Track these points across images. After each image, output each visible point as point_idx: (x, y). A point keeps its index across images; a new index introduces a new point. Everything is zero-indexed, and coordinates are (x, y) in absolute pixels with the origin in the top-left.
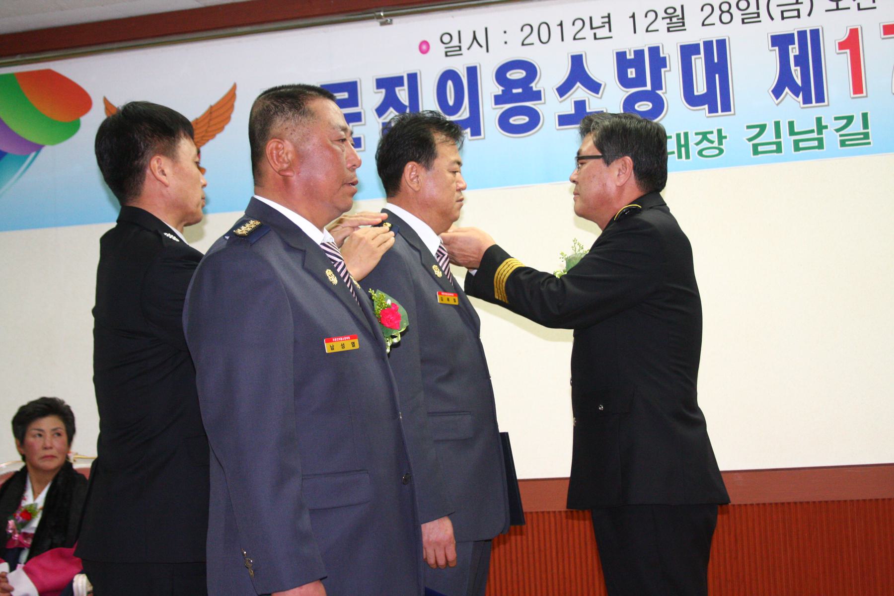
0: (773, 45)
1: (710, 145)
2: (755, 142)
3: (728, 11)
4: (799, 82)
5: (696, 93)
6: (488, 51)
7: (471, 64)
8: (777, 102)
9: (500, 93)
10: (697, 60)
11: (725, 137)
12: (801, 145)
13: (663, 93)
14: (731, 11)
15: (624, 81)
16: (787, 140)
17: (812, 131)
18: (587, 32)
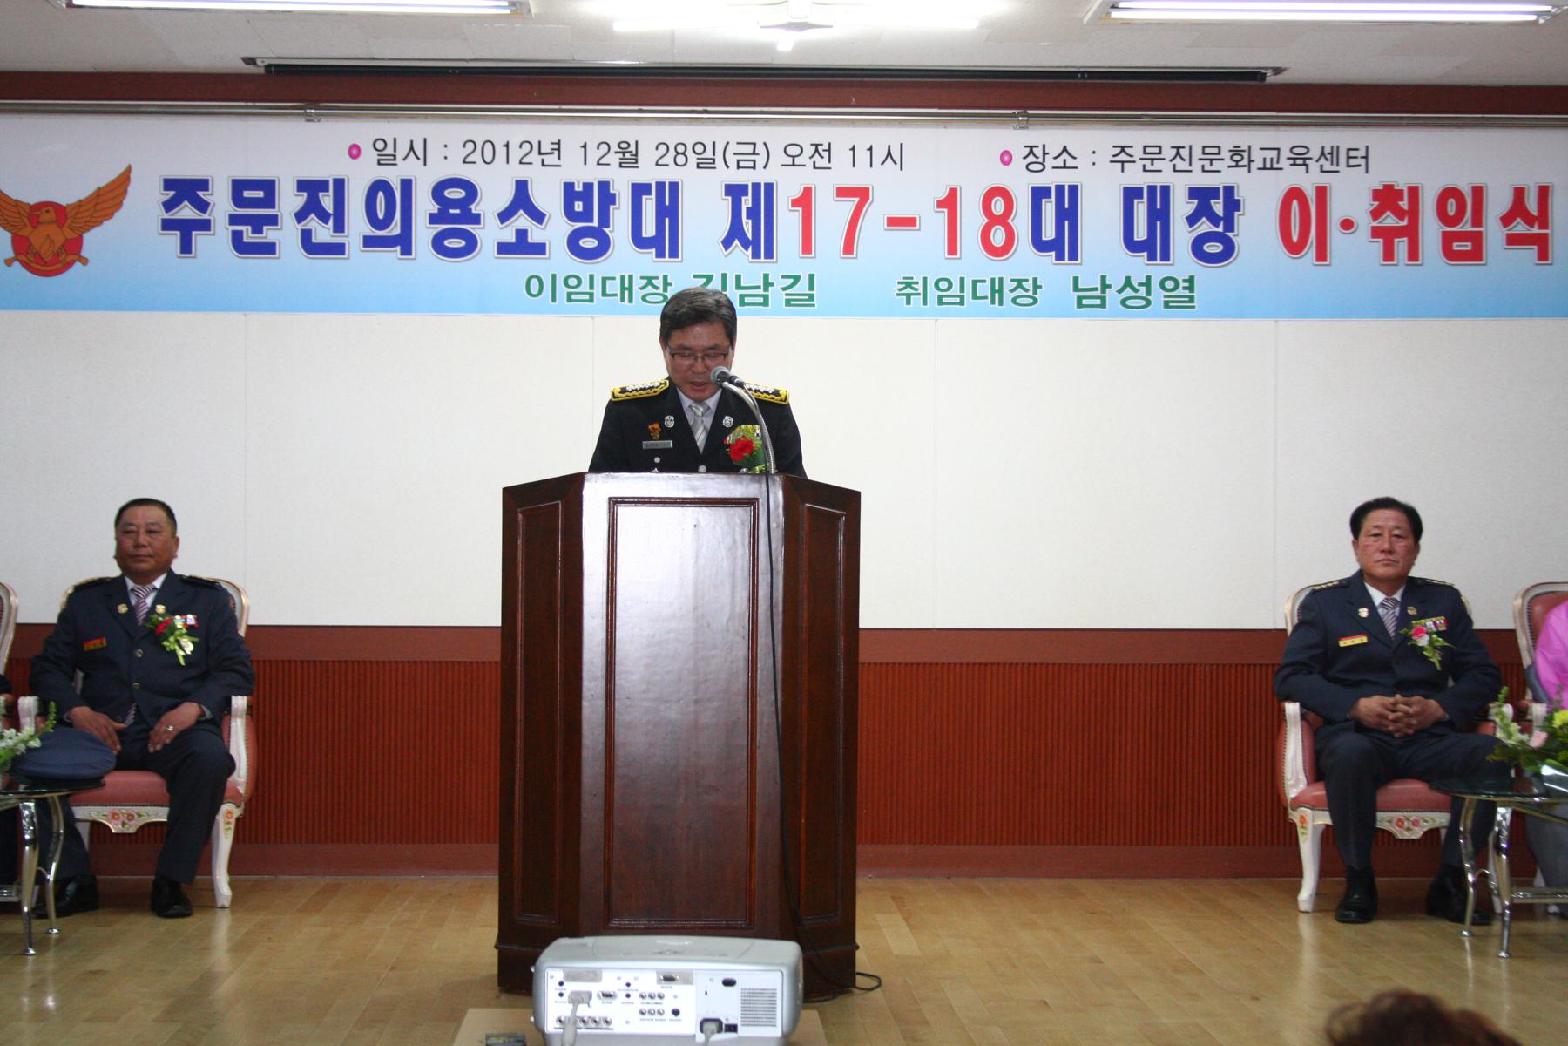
0: (726, 195)
1: (655, 291)
3: (683, 154)
4: (749, 235)
5: (644, 235)
6: (425, 164)
8: (726, 253)
9: (436, 211)
11: (671, 284)
12: (747, 300)
13: (611, 232)
14: (686, 153)
15: (571, 214)
17: (759, 287)
18: (535, 157)
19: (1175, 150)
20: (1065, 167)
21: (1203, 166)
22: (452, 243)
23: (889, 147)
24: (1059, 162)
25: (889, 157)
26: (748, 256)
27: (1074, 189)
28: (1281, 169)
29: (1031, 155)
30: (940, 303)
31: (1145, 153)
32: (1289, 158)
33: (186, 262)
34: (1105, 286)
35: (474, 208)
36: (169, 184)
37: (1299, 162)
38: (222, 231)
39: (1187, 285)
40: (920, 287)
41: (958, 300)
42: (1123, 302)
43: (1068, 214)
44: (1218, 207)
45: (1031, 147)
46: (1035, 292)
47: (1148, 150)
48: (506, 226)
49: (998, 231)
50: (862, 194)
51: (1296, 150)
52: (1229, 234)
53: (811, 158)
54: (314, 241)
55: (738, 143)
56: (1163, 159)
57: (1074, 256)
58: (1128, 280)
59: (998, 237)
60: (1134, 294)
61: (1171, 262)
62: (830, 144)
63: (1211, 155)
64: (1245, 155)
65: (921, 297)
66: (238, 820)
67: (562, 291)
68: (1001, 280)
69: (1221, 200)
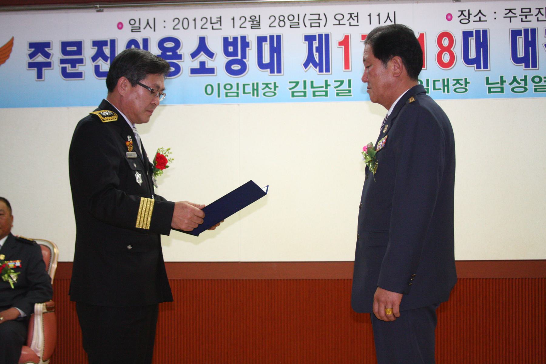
0: (305, 40)
1: (269, 90)
2: (293, 90)
3: (283, 21)
4: (317, 61)
5: (264, 62)
6: (154, 31)
7: (145, 37)
8: (306, 70)
9: (160, 54)
12: (317, 94)
14: (285, 21)
15: (227, 53)
16: (309, 91)
17: (323, 87)
18: (208, 25)
19: (538, 10)
20: (480, 21)
23: (388, 13)
24: (477, 18)
25: (388, 19)
26: (317, 71)
27: (485, 32)
29: (462, 15)
31: (522, 12)
33: (40, 83)
34: (502, 81)
35: (179, 52)
36: (31, 45)
38: (57, 67)
42: (513, 90)
45: (462, 11)
46: (466, 86)
47: (524, 11)
48: (195, 60)
49: (446, 55)
53: (348, 20)
54: (101, 70)
55: (311, 14)
56: (532, 15)
57: (486, 66)
58: (515, 79)
59: (446, 58)
62: (358, 13)
67: (223, 91)
68: (448, 80)
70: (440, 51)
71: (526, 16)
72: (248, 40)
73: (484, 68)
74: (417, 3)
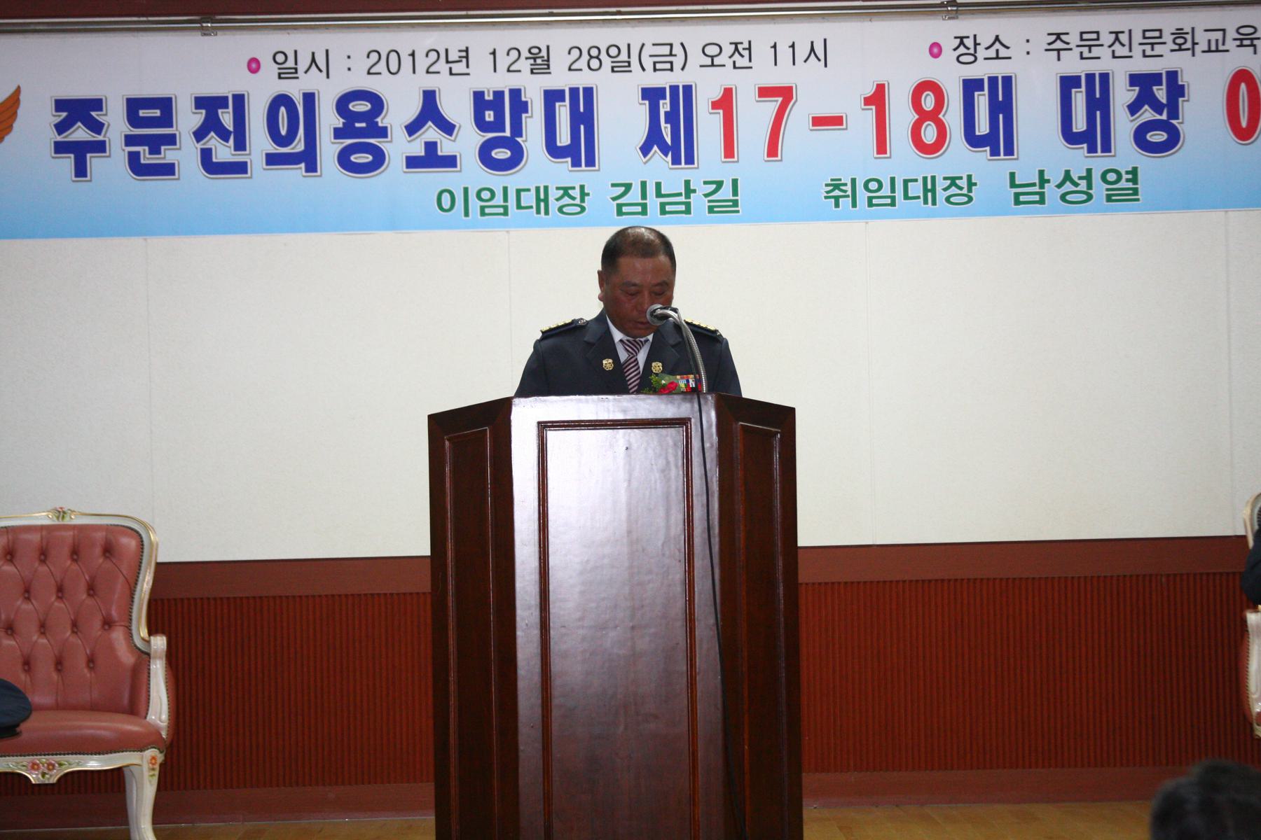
0: (643, 99)
1: (572, 202)
2: (620, 201)
3: (597, 57)
4: (669, 140)
5: (559, 144)
6: (328, 77)
7: (309, 89)
8: (644, 160)
9: (341, 126)
10: (562, 108)
11: (588, 194)
13: (523, 141)
14: (600, 57)
15: (481, 124)
17: (680, 195)
18: (442, 66)
19: (1114, 35)
20: (997, 58)
21: (1144, 51)
22: (358, 158)
23: (812, 43)
24: (992, 53)
25: (812, 54)
26: (668, 162)
27: (1008, 80)
28: (1227, 51)
29: (962, 47)
30: (870, 204)
31: (1082, 40)
32: (1235, 39)
33: (82, 186)
34: (1043, 181)
36: (60, 105)
37: (1247, 42)
38: (118, 152)
39: (1130, 176)
40: (849, 188)
41: (889, 201)
42: (1063, 197)
43: (1003, 107)
44: (1161, 93)
45: (962, 38)
46: (970, 190)
48: (414, 140)
49: (929, 127)
50: (785, 94)
51: (1243, 31)
52: (1174, 122)
53: (730, 57)
56: (1102, 45)
57: (1009, 151)
58: (1067, 176)
60: (1075, 189)
61: (1112, 154)
62: (750, 42)
63: (1152, 38)
64: (1189, 37)
65: (850, 198)
66: (161, 765)
67: (475, 205)
69: (1164, 87)
70: (917, 120)
71: (1090, 46)
72: (525, 97)
73: (1005, 155)
74: (870, 20)
